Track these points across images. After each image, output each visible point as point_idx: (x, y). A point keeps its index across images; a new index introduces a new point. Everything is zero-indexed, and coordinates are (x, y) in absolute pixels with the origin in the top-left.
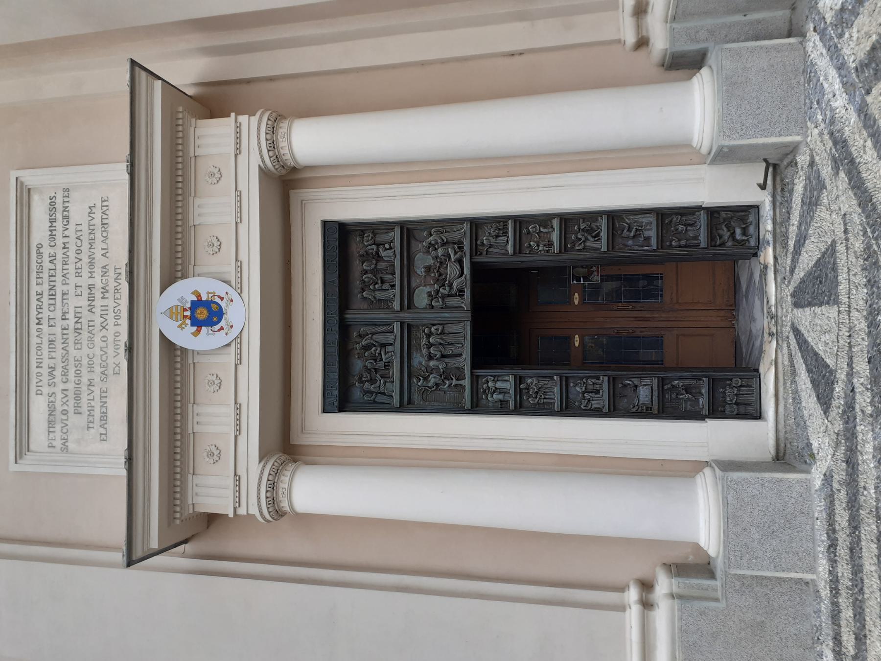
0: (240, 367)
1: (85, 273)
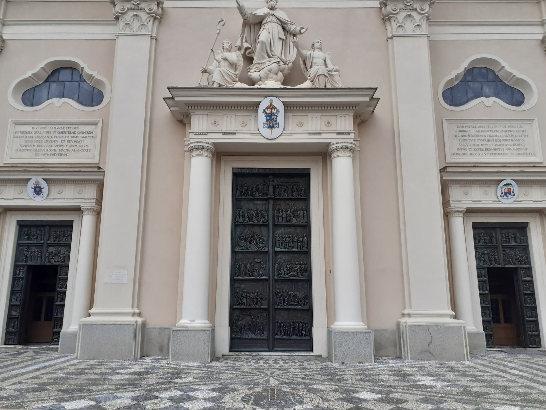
0: (23, 200)
1: (68, 144)
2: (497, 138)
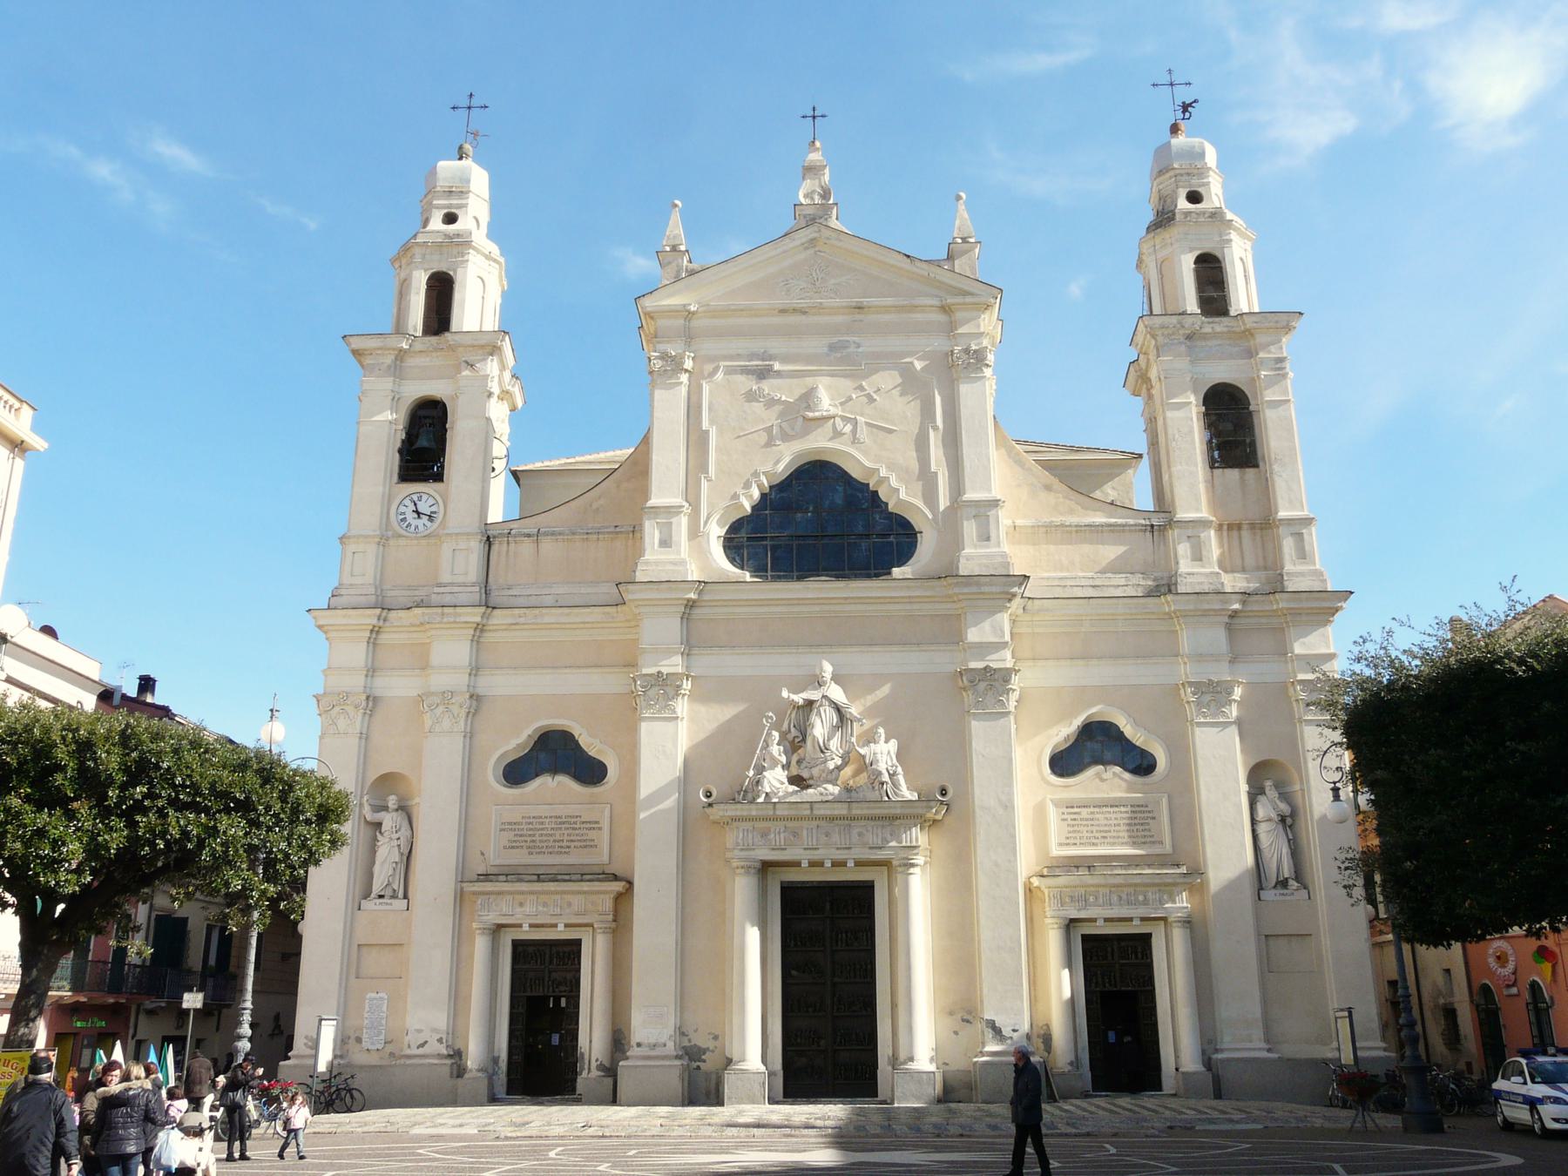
1: (569, 838)
2: (1116, 822)
